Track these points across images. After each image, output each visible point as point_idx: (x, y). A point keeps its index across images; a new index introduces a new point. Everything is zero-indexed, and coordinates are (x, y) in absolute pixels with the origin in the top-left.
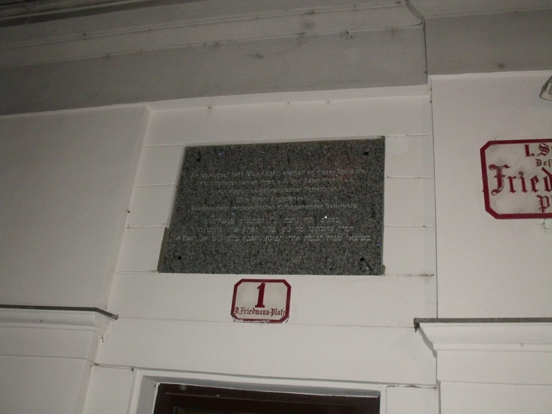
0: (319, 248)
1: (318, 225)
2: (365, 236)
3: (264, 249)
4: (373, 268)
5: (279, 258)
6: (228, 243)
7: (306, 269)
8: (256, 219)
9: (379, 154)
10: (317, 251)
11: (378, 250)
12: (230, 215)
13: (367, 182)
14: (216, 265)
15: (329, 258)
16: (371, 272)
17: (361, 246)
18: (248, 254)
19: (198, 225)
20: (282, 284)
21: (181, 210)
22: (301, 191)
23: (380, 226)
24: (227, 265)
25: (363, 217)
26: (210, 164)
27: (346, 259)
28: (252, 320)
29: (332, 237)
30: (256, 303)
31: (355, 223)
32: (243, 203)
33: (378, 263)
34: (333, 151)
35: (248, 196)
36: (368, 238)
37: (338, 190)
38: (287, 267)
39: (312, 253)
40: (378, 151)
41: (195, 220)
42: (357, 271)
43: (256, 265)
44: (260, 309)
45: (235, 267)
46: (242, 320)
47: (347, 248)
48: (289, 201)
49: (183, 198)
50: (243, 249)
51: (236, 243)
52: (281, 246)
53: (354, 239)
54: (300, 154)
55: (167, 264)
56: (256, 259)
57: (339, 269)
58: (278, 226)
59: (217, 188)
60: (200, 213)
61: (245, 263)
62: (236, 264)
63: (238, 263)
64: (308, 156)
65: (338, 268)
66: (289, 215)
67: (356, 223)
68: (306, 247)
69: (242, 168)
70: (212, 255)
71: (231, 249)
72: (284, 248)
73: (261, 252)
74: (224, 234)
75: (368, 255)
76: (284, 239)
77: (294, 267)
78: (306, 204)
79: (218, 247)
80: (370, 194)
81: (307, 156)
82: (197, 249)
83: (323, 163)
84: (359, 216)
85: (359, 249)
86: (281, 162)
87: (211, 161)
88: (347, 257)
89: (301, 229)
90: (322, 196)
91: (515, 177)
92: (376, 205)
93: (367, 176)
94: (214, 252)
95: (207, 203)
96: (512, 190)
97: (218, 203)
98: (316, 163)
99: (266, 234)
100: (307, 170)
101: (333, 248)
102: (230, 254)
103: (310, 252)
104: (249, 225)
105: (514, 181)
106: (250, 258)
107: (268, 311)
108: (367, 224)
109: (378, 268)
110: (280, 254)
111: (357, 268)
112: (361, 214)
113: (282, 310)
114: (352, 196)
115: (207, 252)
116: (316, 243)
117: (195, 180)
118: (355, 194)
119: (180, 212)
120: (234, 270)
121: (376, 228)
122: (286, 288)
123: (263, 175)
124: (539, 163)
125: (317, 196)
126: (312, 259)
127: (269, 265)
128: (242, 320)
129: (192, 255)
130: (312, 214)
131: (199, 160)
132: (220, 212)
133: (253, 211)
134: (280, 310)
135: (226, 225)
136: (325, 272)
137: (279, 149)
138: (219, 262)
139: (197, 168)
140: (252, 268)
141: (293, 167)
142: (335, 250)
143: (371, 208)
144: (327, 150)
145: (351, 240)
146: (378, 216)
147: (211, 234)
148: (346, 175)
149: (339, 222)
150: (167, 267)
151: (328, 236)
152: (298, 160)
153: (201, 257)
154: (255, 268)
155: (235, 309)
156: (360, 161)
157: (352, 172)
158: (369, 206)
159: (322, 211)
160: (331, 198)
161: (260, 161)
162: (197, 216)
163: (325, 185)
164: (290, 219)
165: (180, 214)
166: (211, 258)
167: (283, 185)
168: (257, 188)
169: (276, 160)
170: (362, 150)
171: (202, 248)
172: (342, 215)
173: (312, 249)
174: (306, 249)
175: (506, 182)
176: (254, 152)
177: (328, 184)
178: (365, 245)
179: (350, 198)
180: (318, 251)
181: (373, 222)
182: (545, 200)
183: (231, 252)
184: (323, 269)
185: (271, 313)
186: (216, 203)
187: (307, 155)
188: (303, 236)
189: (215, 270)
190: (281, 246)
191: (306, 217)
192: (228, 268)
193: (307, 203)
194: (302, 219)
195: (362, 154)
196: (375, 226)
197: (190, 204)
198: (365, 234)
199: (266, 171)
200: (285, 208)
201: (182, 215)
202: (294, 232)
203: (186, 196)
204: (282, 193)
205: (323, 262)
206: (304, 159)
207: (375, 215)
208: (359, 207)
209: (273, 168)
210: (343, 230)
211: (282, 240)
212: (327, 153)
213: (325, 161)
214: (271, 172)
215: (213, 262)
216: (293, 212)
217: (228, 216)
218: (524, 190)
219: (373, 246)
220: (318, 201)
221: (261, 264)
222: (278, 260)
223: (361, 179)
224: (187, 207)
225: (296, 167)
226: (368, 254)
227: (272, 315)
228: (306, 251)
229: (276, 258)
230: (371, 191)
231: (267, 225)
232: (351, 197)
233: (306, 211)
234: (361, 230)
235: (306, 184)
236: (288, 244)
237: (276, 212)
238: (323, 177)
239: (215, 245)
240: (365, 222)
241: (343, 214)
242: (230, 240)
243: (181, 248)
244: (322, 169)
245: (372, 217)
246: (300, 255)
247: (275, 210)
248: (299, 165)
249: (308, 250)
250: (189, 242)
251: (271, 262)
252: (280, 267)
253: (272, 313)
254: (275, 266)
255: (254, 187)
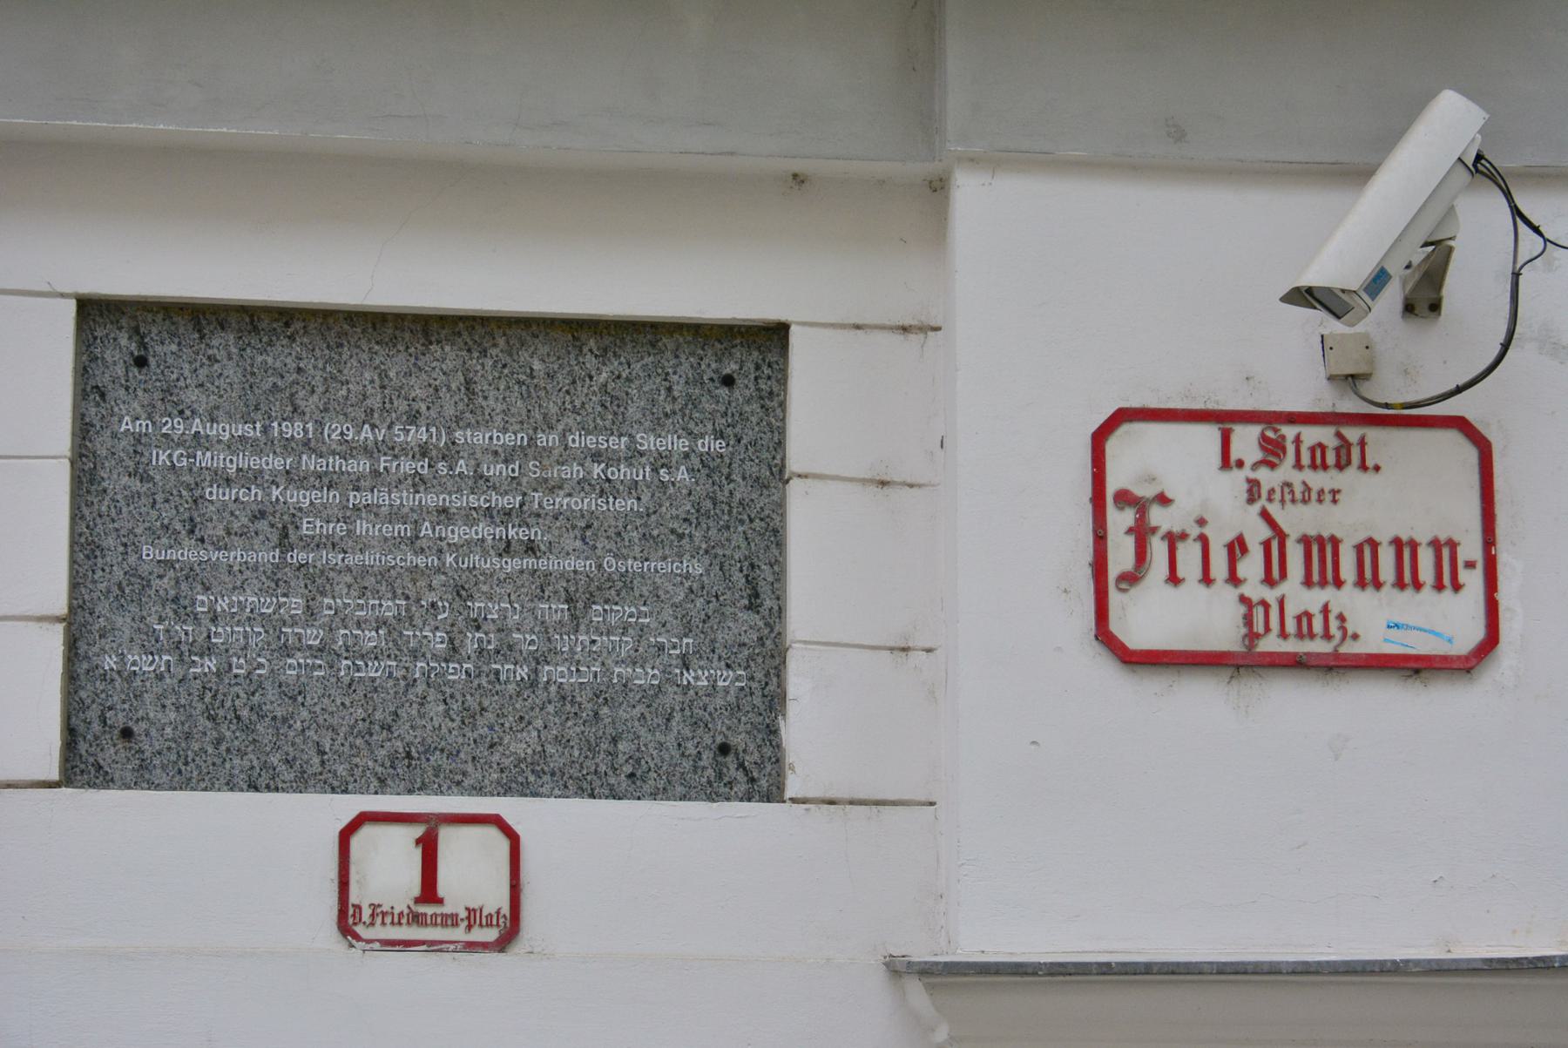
0: (590, 705)
1: (582, 627)
2: (731, 673)
3: (415, 706)
4: (755, 774)
5: (464, 736)
6: (291, 683)
7: (553, 774)
8: (377, 602)
9: (769, 383)
10: (584, 715)
11: (769, 717)
12: (286, 582)
13: (732, 485)
14: (258, 758)
15: (621, 738)
16: (750, 786)
17: (719, 702)
18: (364, 720)
19: (175, 612)
20: (492, 832)
21: (103, 557)
22: (521, 506)
23: (775, 637)
24: (295, 759)
25: (721, 605)
26: (185, 379)
27: (675, 744)
28: (407, 944)
29: (629, 670)
30: (416, 891)
31: (698, 627)
32: (324, 540)
33: (770, 758)
34: (616, 363)
35: (340, 515)
36: (738, 679)
37: (641, 510)
38: (495, 766)
39: (570, 723)
40: (765, 372)
41: (161, 592)
42: (709, 782)
43: (393, 758)
44: (429, 910)
45: (323, 763)
46: (377, 946)
47: (677, 708)
48: (483, 540)
49: (104, 509)
50: (343, 704)
51: (317, 681)
52: (468, 697)
53: (697, 678)
54: (504, 366)
55: (84, 753)
56: (390, 740)
57: (655, 775)
58: (452, 625)
59: (225, 476)
60: (174, 568)
61: (354, 751)
62: (326, 753)
63: (331, 749)
64: (534, 374)
65: (650, 773)
66: (485, 588)
67: (700, 626)
68: (550, 702)
69: (305, 403)
70: (238, 722)
71: (303, 704)
72: (480, 704)
73: (404, 715)
74: (272, 650)
75: (740, 733)
76: (477, 672)
77: (515, 766)
78: (538, 554)
79: (257, 694)
80: (740, 529)
81: (531, 372)
82: (183, 701)
83: (587, 406)
84: (709, 602)
85: (713, 711)
86: (444, 389)
87: (187, 366)
88: (677, 739)
89: (526, 641)
90: (589, 526)
91: (1184, 536)
92: (763, 567)
93: (730, 464)
94: (245, 713)
95: (197, 532)
96: (1174, 579)
97: (236, 534)
98: (564, 403)
99: (415, 655)
100: (535, 429)
101: (634, 707)
102: (302, 722)
103: (564, 717)
104: (356, 619)
105: (1182, 548)
106: (371, 735)
107: (457, 915)
108: (736, 631)
109: (770, 774)
110: (466, 722)
111: (710, 772)
112: (717, 597)
113: (498, 913)
114: (687, 532)
115: (221, 713)
116: (581, 690)
117: (139, 441)
118: (696, 527)
119: (99, 559)
120: (321, 774)
121: (763, 645)
122: (504, 844)
123: (384, 436)
124: (1253, 488)
125: (574, 527)
126: (571, 743)
127: (436, 758)
128: (378, 944)
129: (172, 723)
130: (562, 589)
131: (141, 362)
132: (248, 568)
133: (365, 571)
134: (493, 911)
135: (277, 616)
136: (614, 785)
137: (433, 339)
138: (268, 749)
139: (140, 393)
140: (379, 769)
141: (487, 414)
142: (639, 715)
143: (747, 576)
144: (596, 356)
145: (689, 682)
146: (768, 603)
147: (224, 647)
148: (664, 454)
149: (649, 623)
150: (82, 763)
151: (617, 670)
152: (502, 387)
153: (201, 728)
154: (392, 771)
155: (351, 911)
156: (708, 406)
157: (682, 445)
158: (741, 571)
159: (592, 580)
160: (620, 533)
161: (367, 383)
162: (166, 580)
163: (598, 487)
164: (490, 605)
165: (103, 570)
166: (238, 734)
167: (457, 478)
168: (367, 483)
169: (426, 384)
170: (714, 366)
171: (202, 699)
172: (658, 597)
173: (568, 707)
174: (550, 708)
175: (1158, 548)
176: (340, 345)
177: (607, 485)
178: (731, 698)
179: (681, 536)
180: (588, 715)
181: (753, 624)
182: (1259, 613)
183: (305, 714)
184: (606, 774)
185: (466, 923)
186: (229, 533)
187: (532, 369)
188: (538, 663)
189: (256, 774)
190: (468, 697)
191: (541, 598)
192: (302, 767)
193: (543, 548)
194: (530, 605)
195: (712, 379)
196: (760, 639)
197: (131, 531)
198: (729, 662)
199: (392, 423)
200: (471, 566)
201: (110, 573)
202: (507, 651)
203: (113, 500)
204: (457, 508)
205: (604, 751)
206: (519, 382)
207: (758, 601)
208: (708, 571)
209: (418, 412)
210: (661, 648)
211: (470, 676)
212: (598, 369)
213: (594, 398)
214: (413, 428)
215: (247, 747)
216: (498, 579)
217: (277, 586)
218: (1207, 579)
219: (754, 705)
220: (578, 543)
221: (409, 755)
222: (462, 744)
223: (712, 471)
224: (125, 545)
225: (498, 414)
226: (742, 728)
227: (470, 927)
228: (548, 713)
229: (457, 737)
230: (745, 517)
231: (418, 622)
232: (684, 534)
233: (539, 577)
234: (716, 650)
235: (535, 479)
236: (491, 691)
237: (443, 577)
238: (589, 459)
239: (246, 687)
240: (731, 624)
241: (661, 593)
242: (294, 673)
243: (123, 697)
244: (583, 429)
245: (749, 608)
246: (531, 727)
247: (438, 571)
248: (504, 407)
249: (556, 712)
250: (152, 675)
251: (442, 750)
252: (470, 764)
253: (469, 922)
254: (454, 764)
255: (358, 480)
